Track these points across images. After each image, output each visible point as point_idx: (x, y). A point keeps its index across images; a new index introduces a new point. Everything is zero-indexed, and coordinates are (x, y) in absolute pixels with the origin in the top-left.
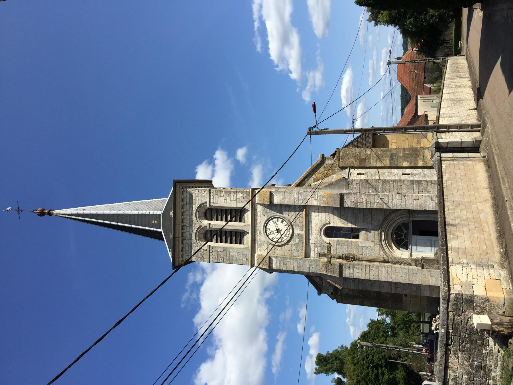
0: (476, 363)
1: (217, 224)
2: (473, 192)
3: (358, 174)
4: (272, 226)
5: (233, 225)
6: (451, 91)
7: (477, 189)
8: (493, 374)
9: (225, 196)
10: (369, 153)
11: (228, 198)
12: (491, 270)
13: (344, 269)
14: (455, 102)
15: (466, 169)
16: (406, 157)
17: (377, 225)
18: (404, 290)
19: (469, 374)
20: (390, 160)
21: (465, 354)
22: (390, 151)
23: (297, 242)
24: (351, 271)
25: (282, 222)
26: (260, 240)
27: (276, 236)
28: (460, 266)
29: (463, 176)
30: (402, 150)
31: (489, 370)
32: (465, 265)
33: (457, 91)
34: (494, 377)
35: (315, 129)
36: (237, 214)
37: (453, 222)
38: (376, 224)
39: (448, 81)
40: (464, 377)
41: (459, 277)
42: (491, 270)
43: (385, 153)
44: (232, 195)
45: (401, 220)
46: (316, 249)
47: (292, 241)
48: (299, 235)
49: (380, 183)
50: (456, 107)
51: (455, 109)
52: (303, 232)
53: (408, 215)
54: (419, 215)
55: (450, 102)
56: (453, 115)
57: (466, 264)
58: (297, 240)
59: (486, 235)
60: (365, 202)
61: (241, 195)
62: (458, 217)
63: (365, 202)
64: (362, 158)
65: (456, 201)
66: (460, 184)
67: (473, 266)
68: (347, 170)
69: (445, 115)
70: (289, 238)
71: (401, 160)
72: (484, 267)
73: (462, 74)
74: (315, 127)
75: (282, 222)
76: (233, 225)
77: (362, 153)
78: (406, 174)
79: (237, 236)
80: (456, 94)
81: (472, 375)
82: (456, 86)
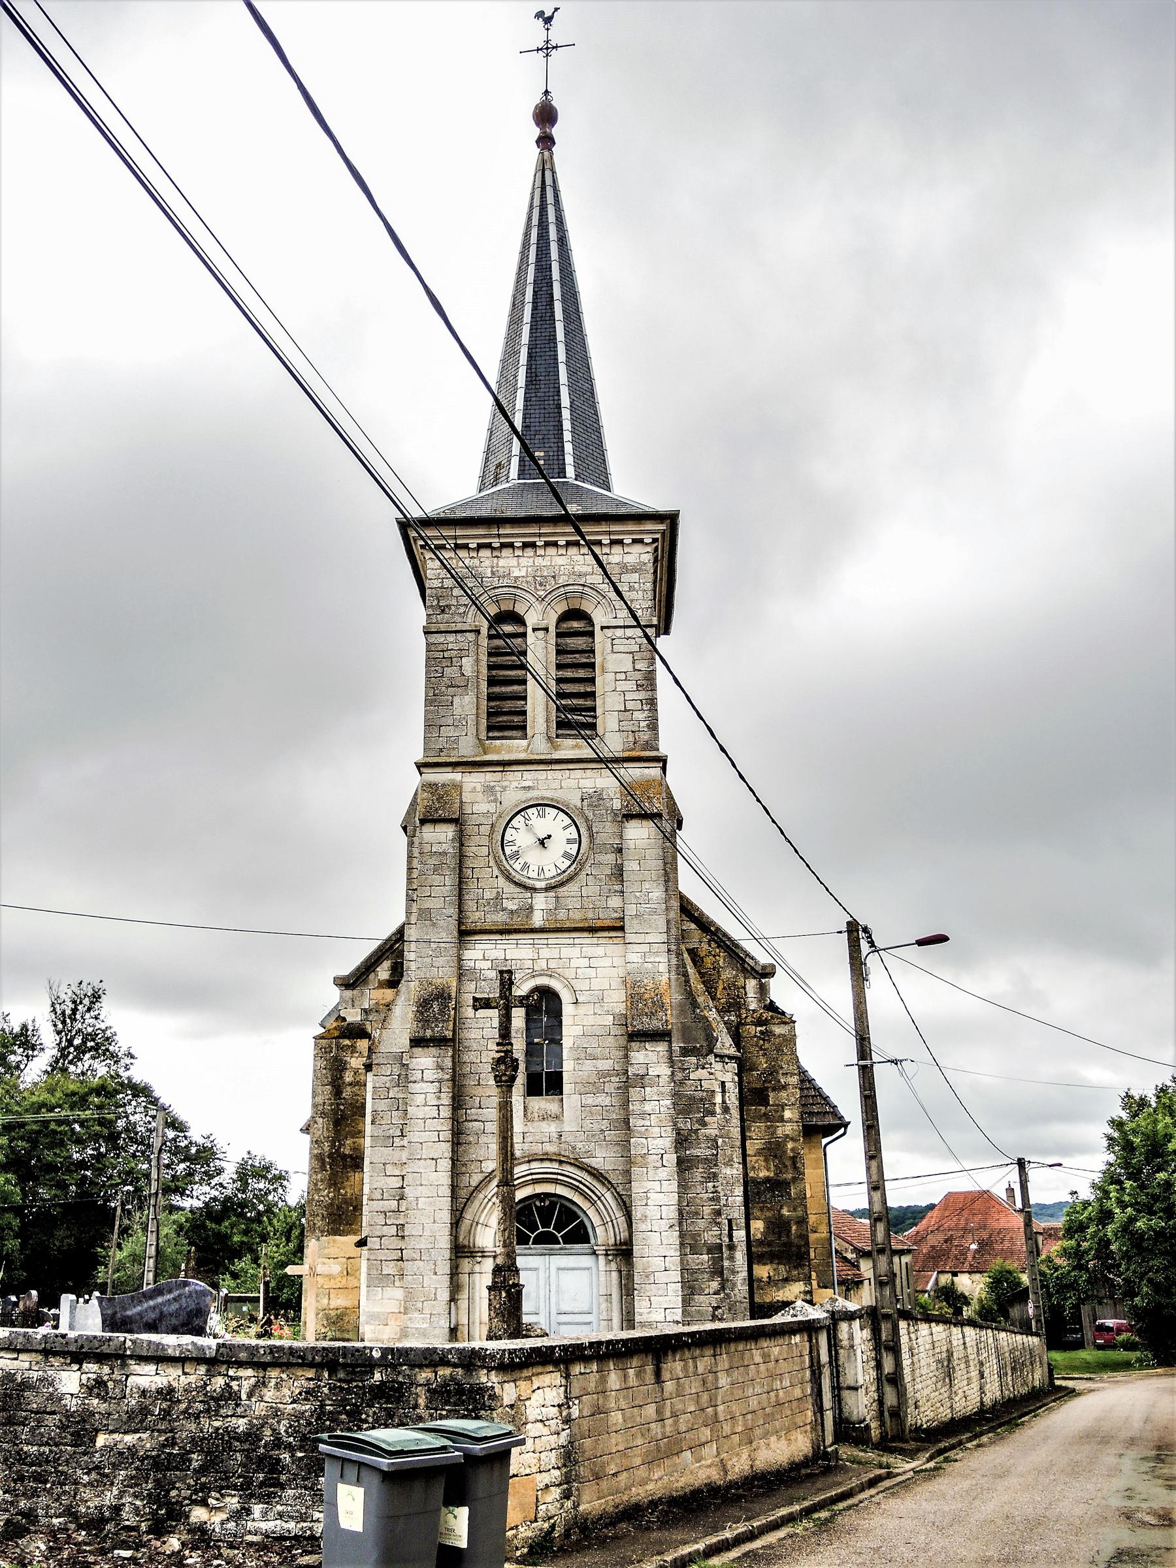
0: (286, 1457)
1: (540, 653)
2: (739, 1429)
3: (723, 1083)
4: (553, 824)
5: (538, 706)
6: (969, 1350)
7: (748, 1439)
8: (257, 1509)
9: (638, 675)
10: (787, 1114)
11: (631, 685)
12: (558, 1490)
13: (433, 1051)
14: (945, 1364)
15: (795, 1404)
16: (778, 1226)
17: (574, 1148)
18: (381, 1237)
19: (252, 1436)
20: (767, 1180)
21: (309, 1424)
22: (794, 1179)
23: (506, 903)
24: (429, 1075)
25: (566, 855)
26: (505, 788)
27: (520, 837)
28: (562, 1400)
29: (777, 1396)
30: (800, 1213)
31: (269, 1495)
32: (564, 1414)
33: (972, 1368)
34: (249, 1512)
35: (864, 946)
36: (576, 714)
37: (666, 1375)
38: (579, 1145)
39: (991, 1340)
40: (242, 1421)
41: (534, 1396)
42: (558, 1490)
43: (788, 1163)
44: (642, 695)
45: (596, 1220)
46: (489, 964)
47: (510, 889)
48: (531, 908)
49: (708, 1152)
50: (934, 1366)
51: (929, 1365)
52: (538, 920)
53: (611, 1241)
54: (615, 1275)
55: (944, 1349)
56: (915, 1358)
57: (569, 1414)
58: (511, 905)
59: (642, 1472)
60: (648, 1107)
61: (643, 724)
62: (678, 1384)
63: (648, 1107)
64: (771, 1094)
65: (717, 1379)
66: (758, 1390)
67: (563, 1439)
68: (732, 1051)
69: (913, 1336)
70: (517, 877)
71: (769, 1214)
72: (564, 1470)
73: (1009, 1378)
74: (872, 944)
75: (566, 855)
76: (538, 706)
77: (783, 1094)
78: (731, 1229)
79: (505, 717)
80: (963, 1366)
81: (246, 1447)
82: (981, 1364)
